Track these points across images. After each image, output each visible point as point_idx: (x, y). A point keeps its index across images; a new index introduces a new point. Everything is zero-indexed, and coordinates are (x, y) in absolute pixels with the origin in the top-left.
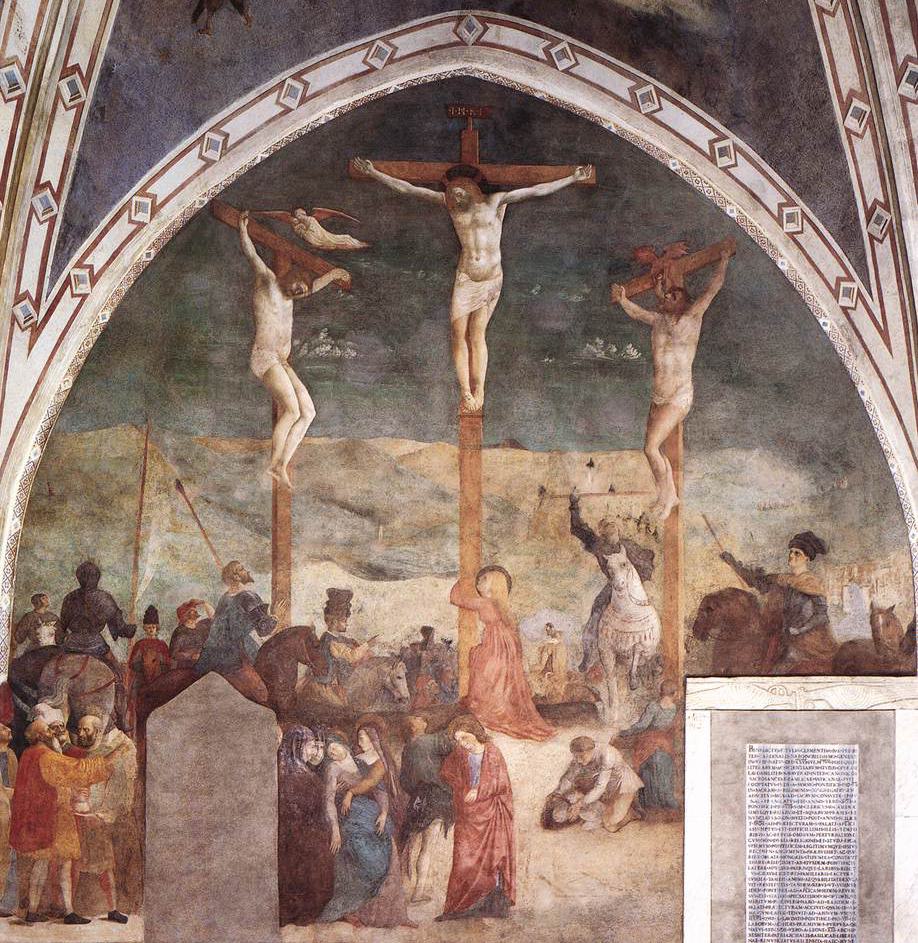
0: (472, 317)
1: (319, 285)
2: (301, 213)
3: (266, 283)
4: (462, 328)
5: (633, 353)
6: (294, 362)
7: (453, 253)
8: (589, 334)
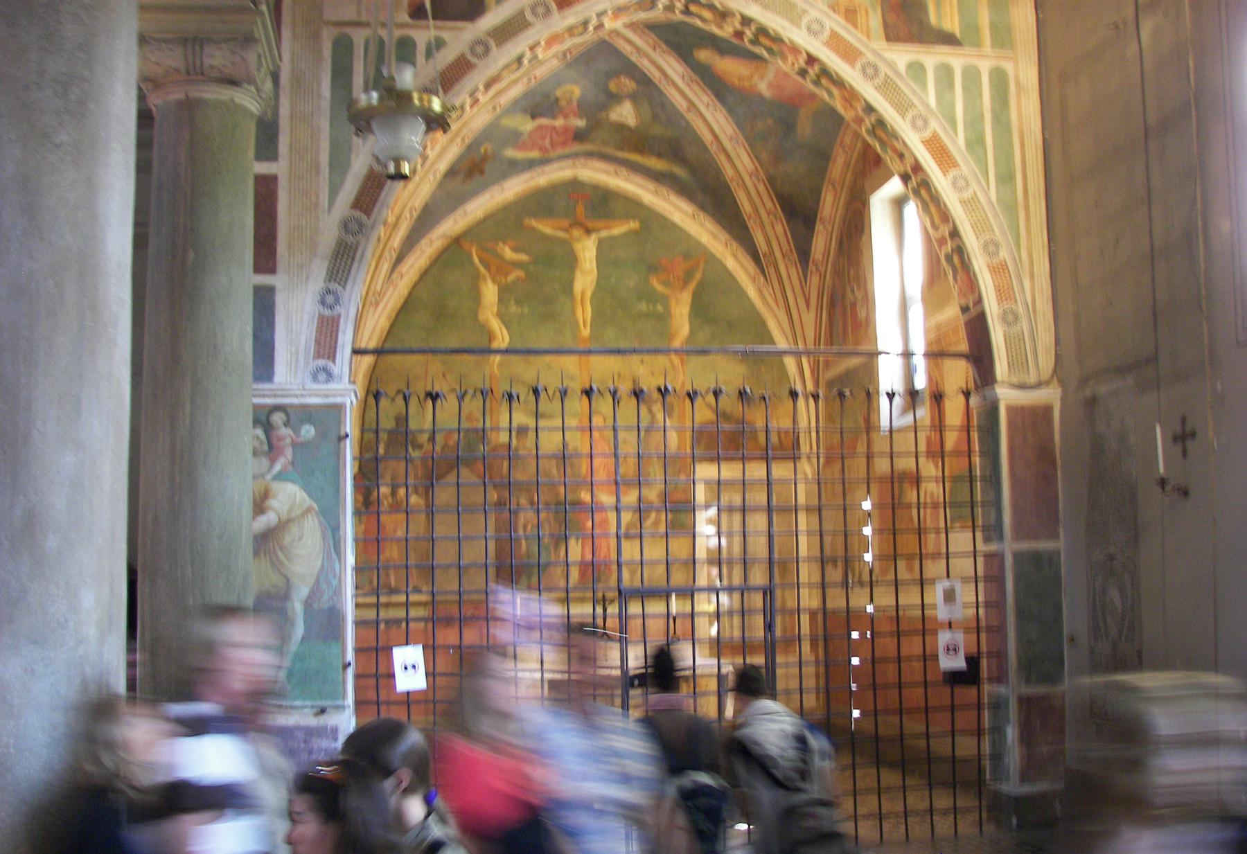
0: (583, 293)
1: (511, 278)
2: (501, 244)
3: (485, 279)
4: (578, 298)
5: (660, 308)
6: (500, 315)
7: (571, 262)
8: (639, 299)
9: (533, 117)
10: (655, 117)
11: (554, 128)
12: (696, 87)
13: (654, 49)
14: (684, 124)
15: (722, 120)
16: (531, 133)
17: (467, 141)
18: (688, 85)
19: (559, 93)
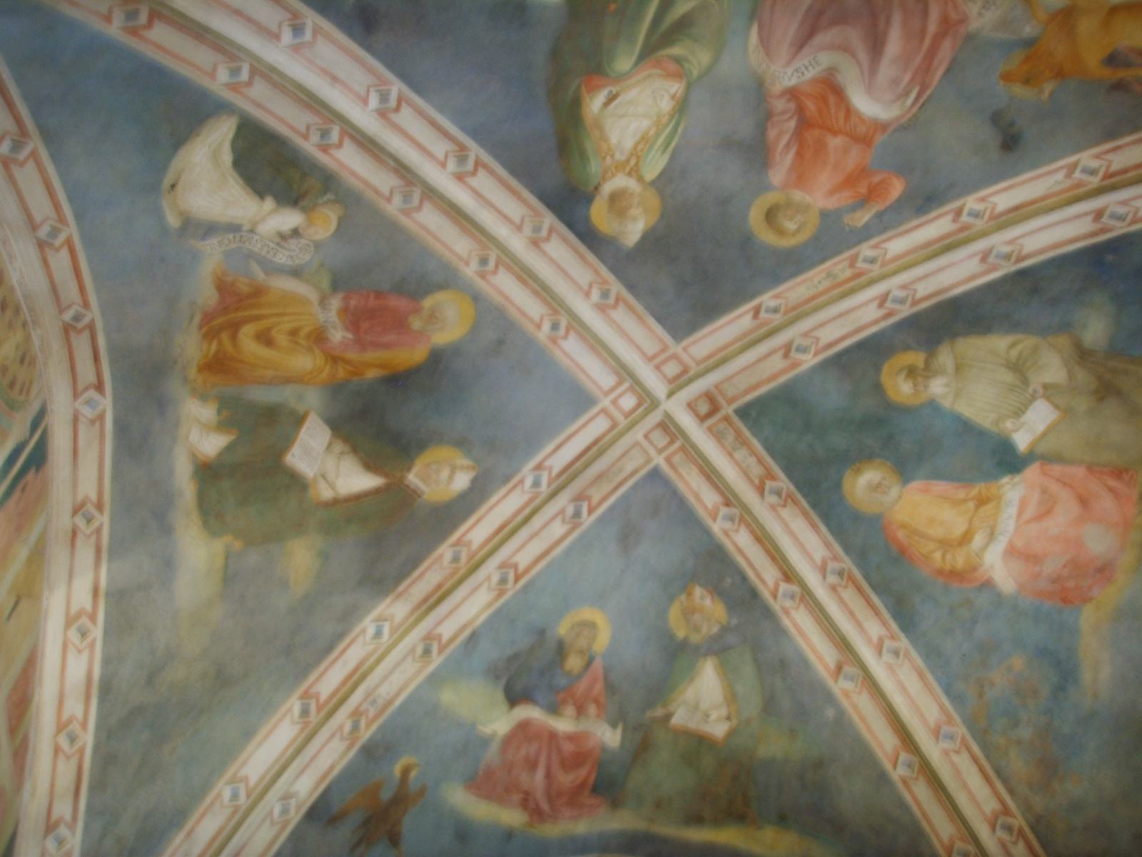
9: (514, 698)
10: (769, 706)
11: (553, 736)
12: (849, 594)
13: (761, 490)
14: (830, 713)
15: (914, 685)
16: (508, 740)
17: (366, 735)
18: (833, 588)
19: (563, 629)
